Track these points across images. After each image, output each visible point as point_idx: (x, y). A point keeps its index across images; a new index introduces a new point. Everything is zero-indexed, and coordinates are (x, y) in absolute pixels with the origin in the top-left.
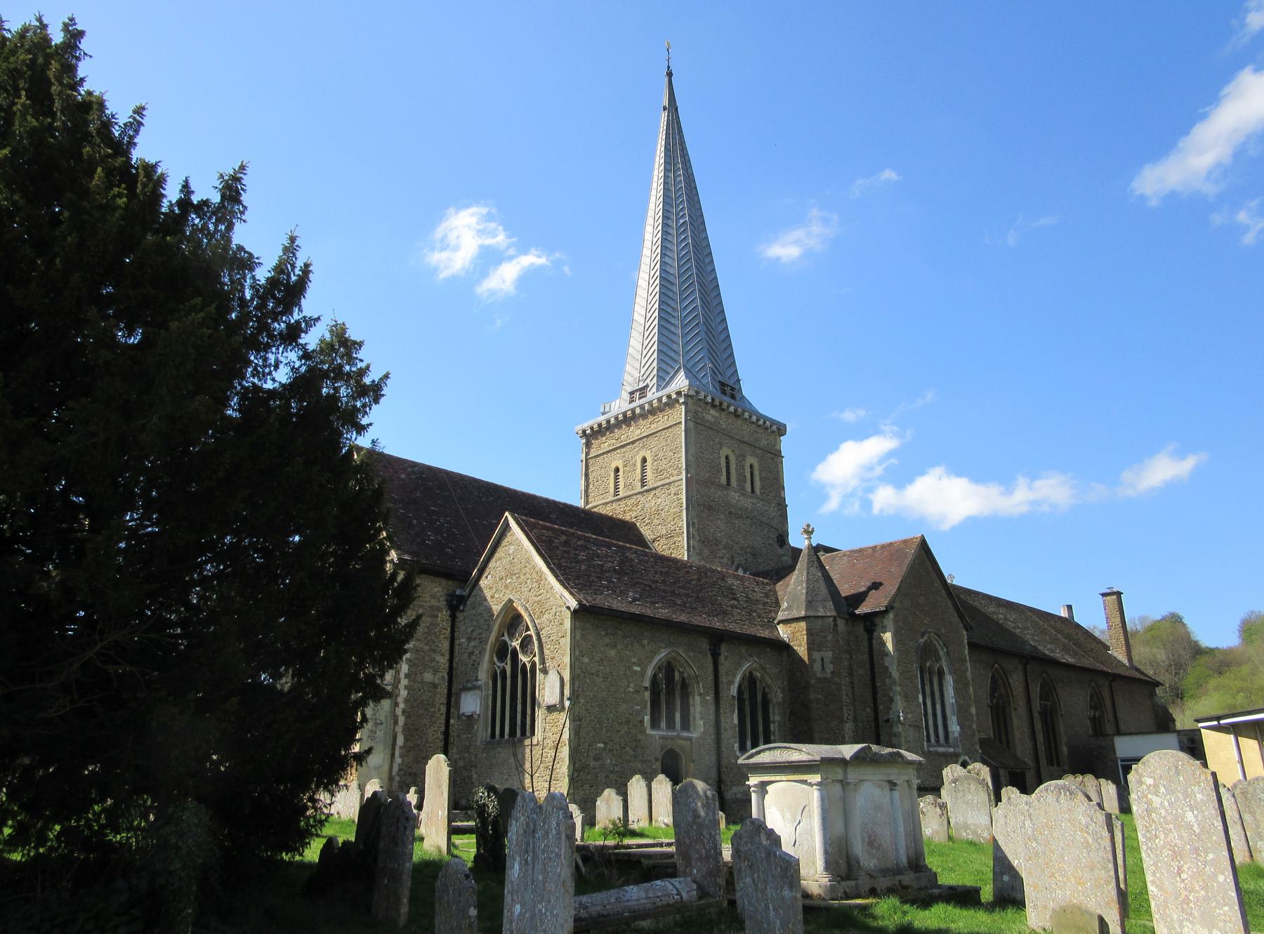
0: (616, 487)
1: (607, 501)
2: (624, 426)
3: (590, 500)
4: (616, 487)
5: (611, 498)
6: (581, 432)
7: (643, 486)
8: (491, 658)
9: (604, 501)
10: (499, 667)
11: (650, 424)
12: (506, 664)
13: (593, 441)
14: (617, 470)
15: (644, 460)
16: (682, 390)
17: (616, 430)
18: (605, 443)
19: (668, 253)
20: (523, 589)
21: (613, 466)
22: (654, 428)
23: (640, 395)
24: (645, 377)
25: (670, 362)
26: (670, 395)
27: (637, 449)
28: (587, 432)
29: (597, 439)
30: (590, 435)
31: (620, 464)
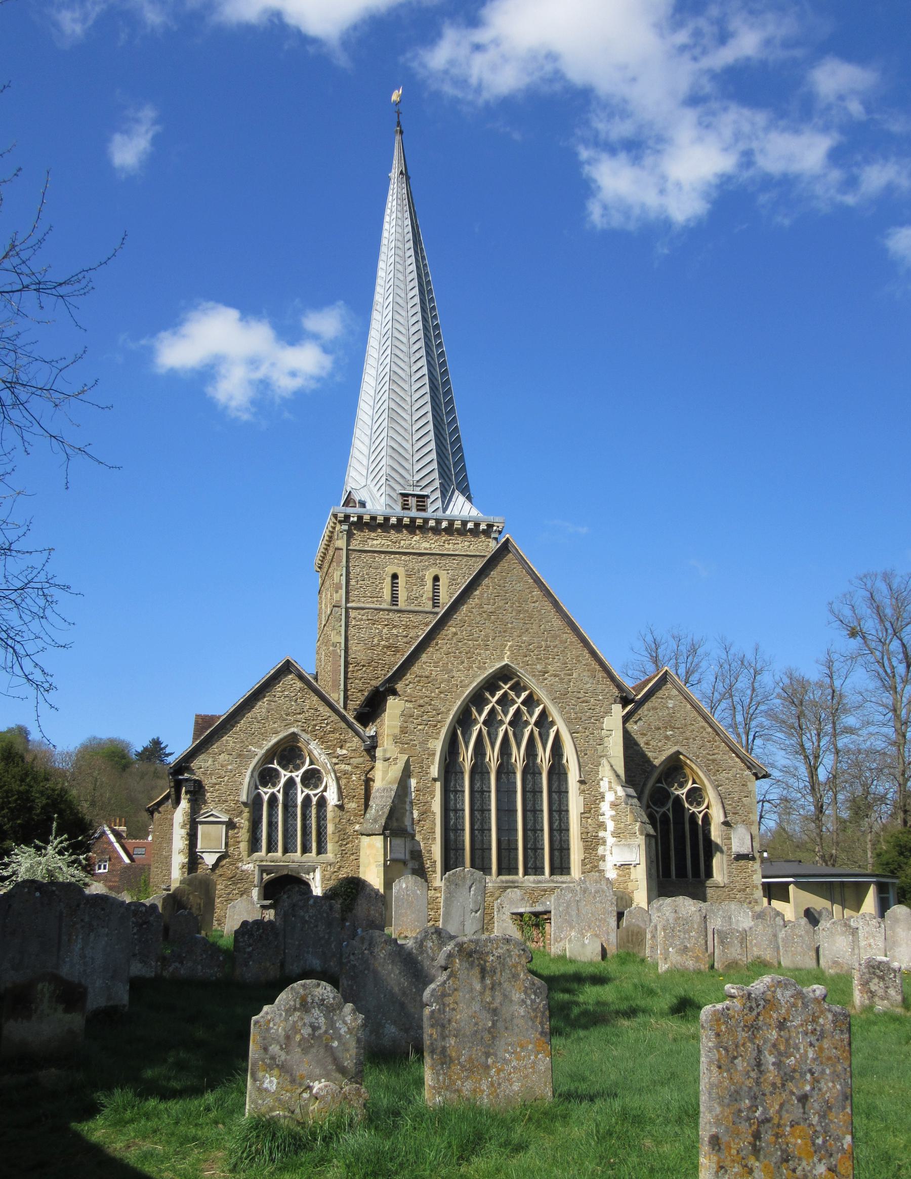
0: (394, 599)
1: (381, 607)
2: (405, 532)
3: (351, 598)
4: (394, 599)
5: (384, 606)
6: (342, 515)
7: (434, 606)
8: (648, 802)
9: (378, 606)
10: (657, 812)
11: (444, 543)
12: (668, 810)
13: (355, 532)
14: (395, 577)
15: (436, 579)
16: (495, 524)
17: (393, 532)
18: (377, 541)
19: (430, 352)
20: (691, 746)
21: (390, 570)
22: (449, 548)
23: (417, 501)
24: (423, 483)
25: (447, 479)
26: (479, 524)
27: (427, 563)
28: (352, 519)
29: (362, 531)
30: (353, 523)
31: (401, 572)
